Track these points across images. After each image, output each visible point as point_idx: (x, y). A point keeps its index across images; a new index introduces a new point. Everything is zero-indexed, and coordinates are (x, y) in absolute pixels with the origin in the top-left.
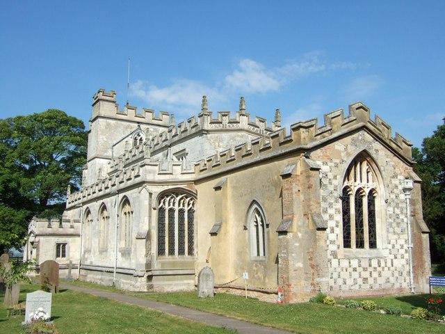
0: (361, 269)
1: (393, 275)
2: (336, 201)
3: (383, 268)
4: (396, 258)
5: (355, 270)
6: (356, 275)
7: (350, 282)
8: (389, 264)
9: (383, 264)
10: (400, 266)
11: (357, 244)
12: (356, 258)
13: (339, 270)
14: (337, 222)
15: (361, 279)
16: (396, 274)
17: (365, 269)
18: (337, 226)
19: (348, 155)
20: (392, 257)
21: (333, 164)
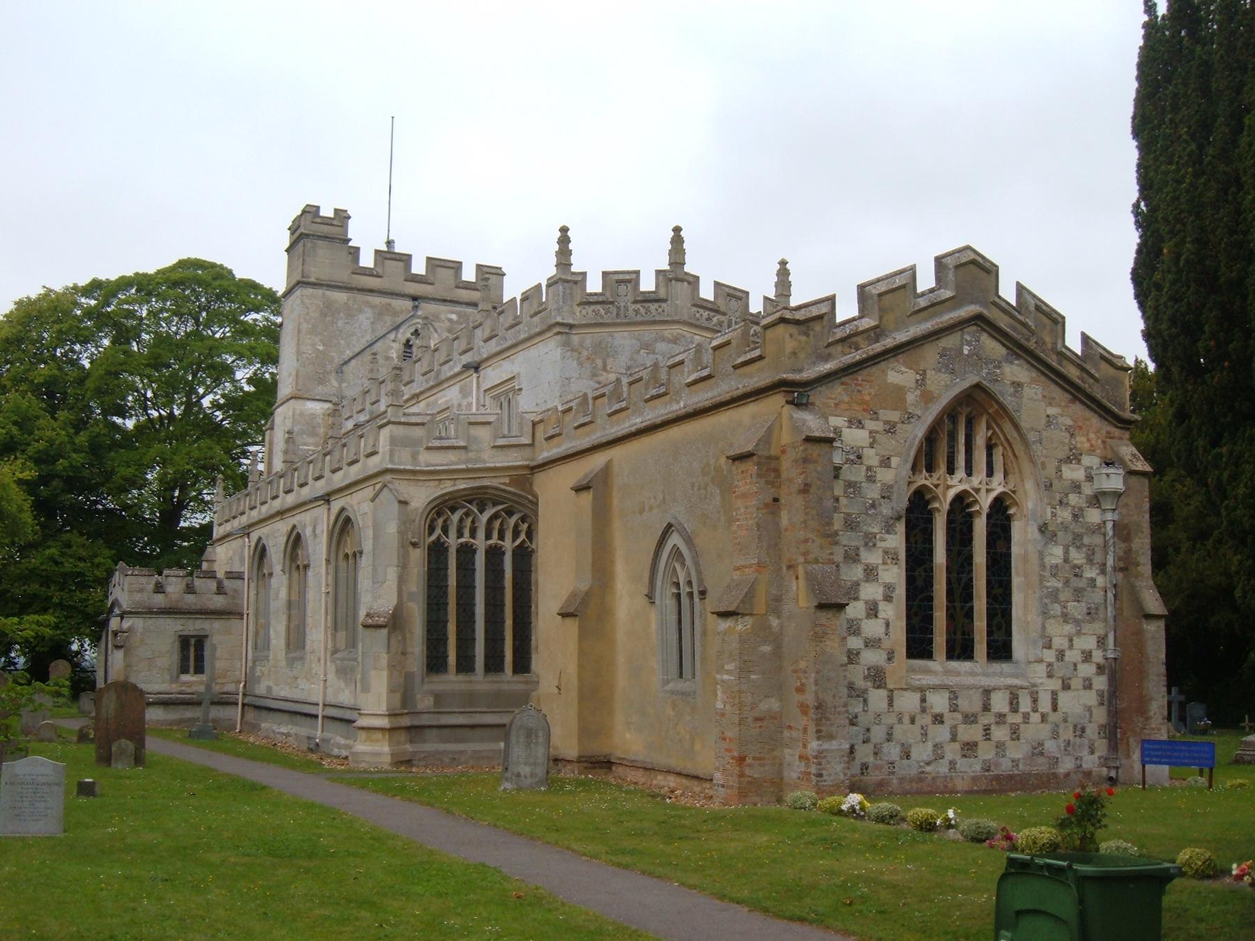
0: (927, 719)
1: (1055, 735)
2: (889, 529)
3: (1026, 716)
4: (1066, 687)
5: (938, 719)
6: (941, 733)
7: (922, 752)
8: (1045, 705)
9: (1025, 704)
10: (1078, 710)
11: (486, 665)
12: (910, 688)
13: (891, 719)
14: (889, 588)
15: (957, 746)
16: (1067, 734)
17: (970, 719)
18: (888, 598)
19: (927, 398)
20: (1055, 684)
21: (878, 426)
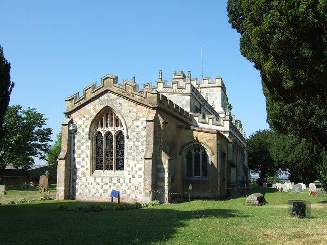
1: (130, 189)
2: (87, 142)
3: (121, 184)
4: (133, 177)
5: (98, 184)
6: (98, 187)
7: (93, 191)
8: (127, 181)
9: (121, 180)
10: (137, 183)
13: (86, 184)
14: (87, 154)
15: (102, 190)
16: (133, 188)
17: (106, 184)
18: (87, 157)
19: (95, 111)
20: (130, 176)
21: (85, 119)
